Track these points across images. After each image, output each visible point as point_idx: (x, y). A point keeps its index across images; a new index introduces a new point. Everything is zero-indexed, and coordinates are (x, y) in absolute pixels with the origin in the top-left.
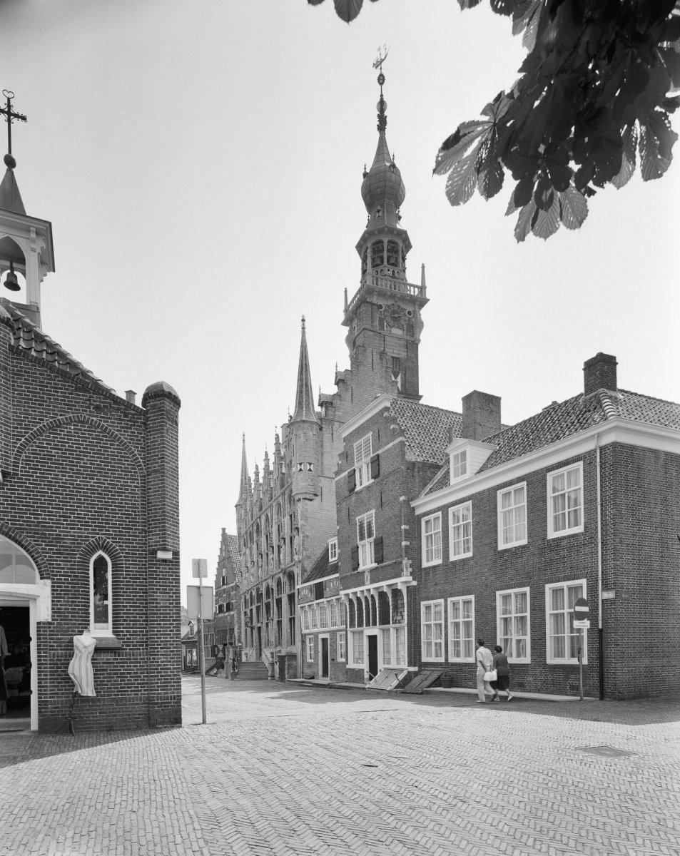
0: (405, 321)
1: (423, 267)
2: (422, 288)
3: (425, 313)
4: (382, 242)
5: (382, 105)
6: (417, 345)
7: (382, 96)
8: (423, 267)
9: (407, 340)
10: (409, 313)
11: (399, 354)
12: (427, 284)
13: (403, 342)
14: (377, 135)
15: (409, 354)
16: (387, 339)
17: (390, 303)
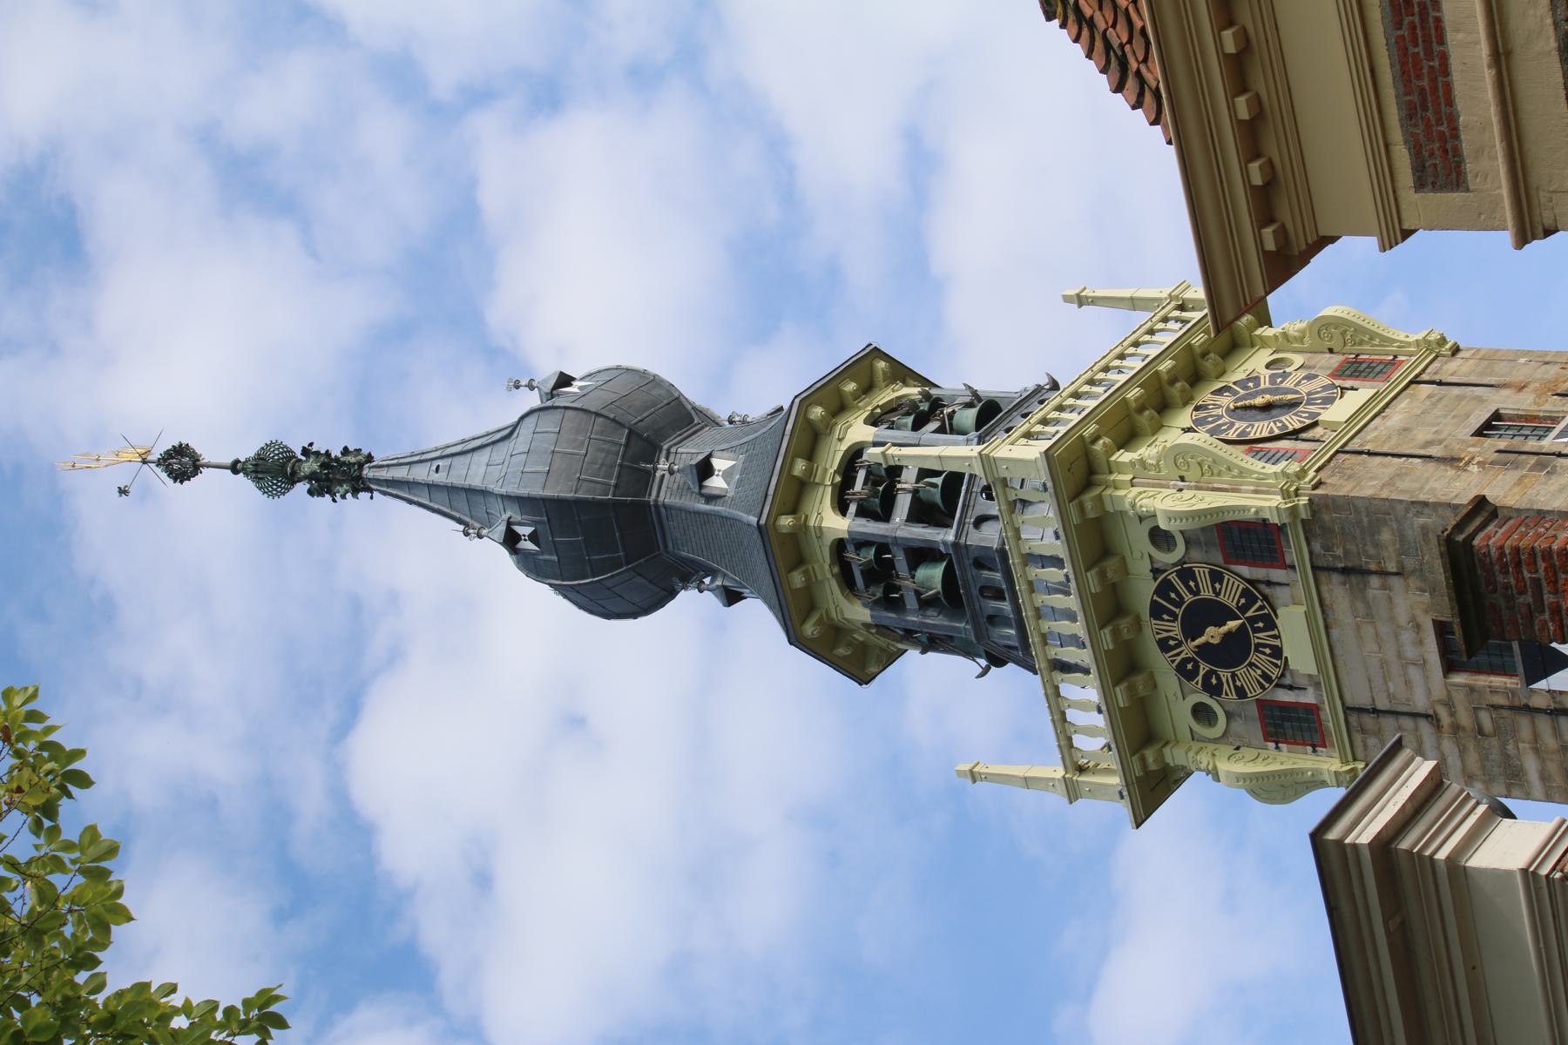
0: (1216, 577)
11: (1418, 627)
13: (1338, 592)
15: (1392, 567)
16: (1359, 697)
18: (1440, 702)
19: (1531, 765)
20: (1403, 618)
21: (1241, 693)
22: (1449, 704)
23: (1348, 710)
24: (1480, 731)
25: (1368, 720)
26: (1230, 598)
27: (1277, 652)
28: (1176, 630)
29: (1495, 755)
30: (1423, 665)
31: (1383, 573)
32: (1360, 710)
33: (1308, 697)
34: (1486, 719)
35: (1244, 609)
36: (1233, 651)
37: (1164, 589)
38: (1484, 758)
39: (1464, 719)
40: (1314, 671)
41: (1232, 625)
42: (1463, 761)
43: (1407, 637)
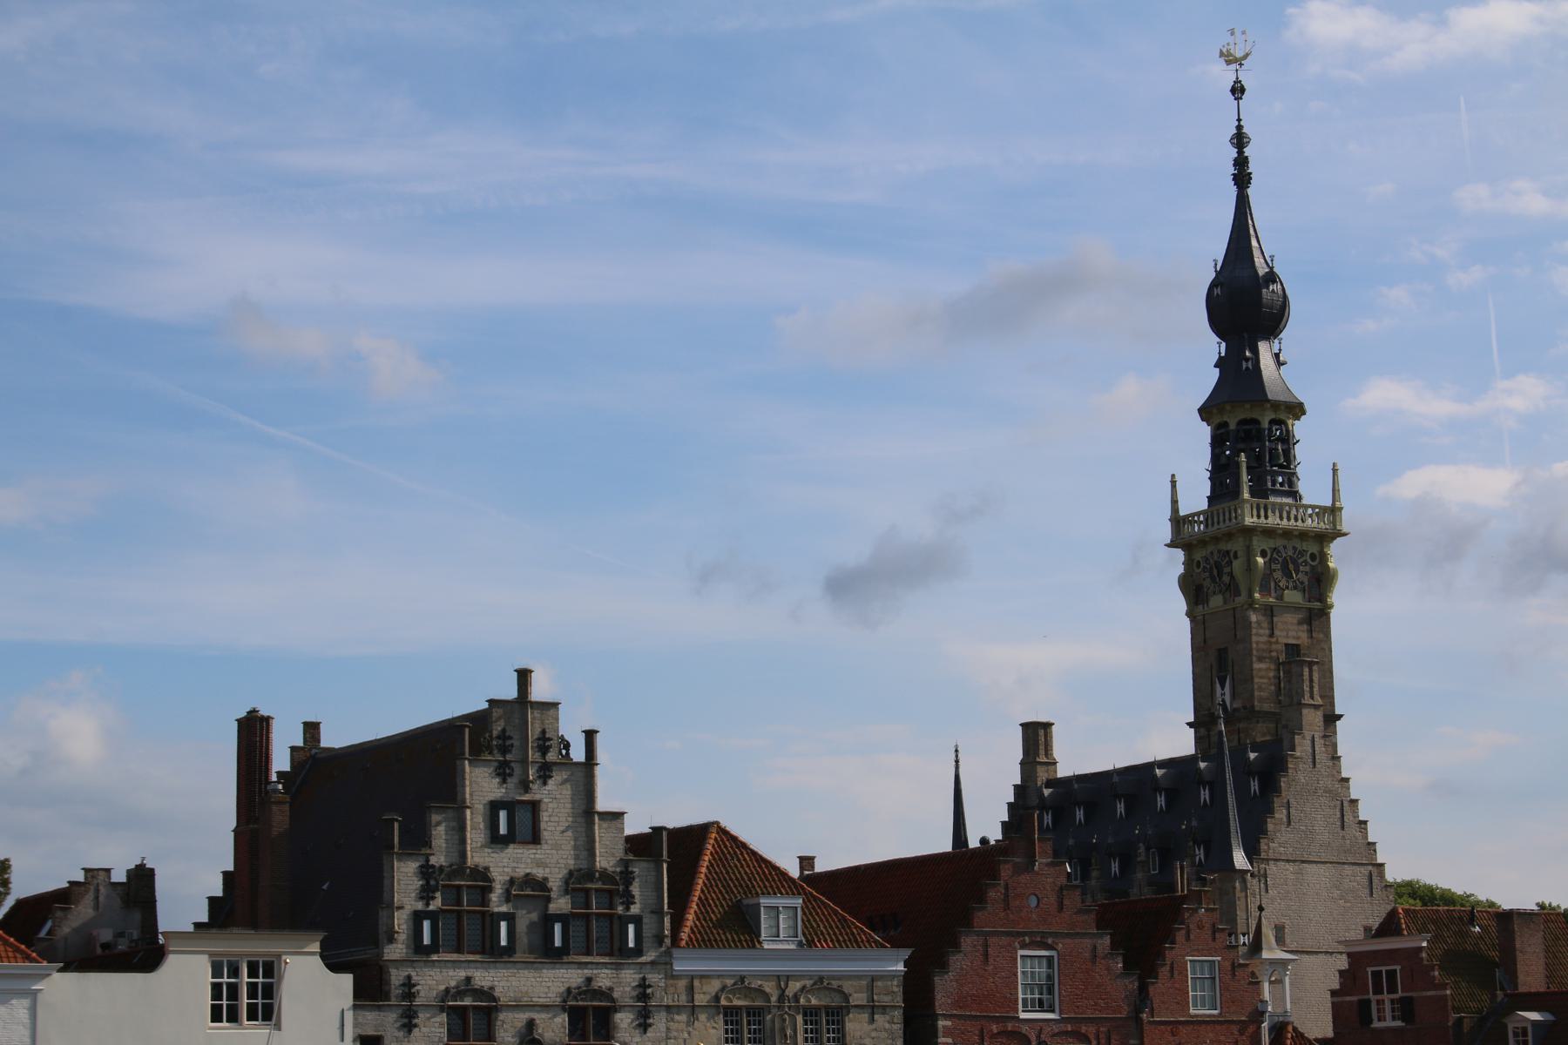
0: (1306, 573)
1: (1335, 471)
2: (1334, 511)
3: (1336, 553)
4: (1256, 422)
5: (1240, 140)
6: (1327, 616)
7: (1239, 120)
8: (1335, 471)
9: (1310, 610)
10: (1313, 557)
11: (1298, 638)
12: (1344, 502)
14: (1233, 191)
15: (1314, 635)
17: (1279, 543)
18: (1277, 640)
19: (1262, 666)
20: (1300, 634)
21: (1274, 570)
22: (1277, 642)
23: (1272, 606)
24: (1271, 651)
25: (1269, 613)
26: (1300, 575)
27: (1287, 588)
28: (1290, 553)
29: (1265, 655)
30: (1287, 637)
31: (1310, 631)
32: (1272, 611)
33: (1273, 594)
34: (1274, 654)
35: (1298, 580)
36: (1289, 576)
37: (1302, 553)
38: (1263, 650)
39: (1274, 647)
40: (1286, 599)
41: (1294, 576)
42: (1262, 642)
43: (1294, 634)
